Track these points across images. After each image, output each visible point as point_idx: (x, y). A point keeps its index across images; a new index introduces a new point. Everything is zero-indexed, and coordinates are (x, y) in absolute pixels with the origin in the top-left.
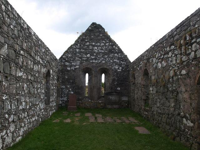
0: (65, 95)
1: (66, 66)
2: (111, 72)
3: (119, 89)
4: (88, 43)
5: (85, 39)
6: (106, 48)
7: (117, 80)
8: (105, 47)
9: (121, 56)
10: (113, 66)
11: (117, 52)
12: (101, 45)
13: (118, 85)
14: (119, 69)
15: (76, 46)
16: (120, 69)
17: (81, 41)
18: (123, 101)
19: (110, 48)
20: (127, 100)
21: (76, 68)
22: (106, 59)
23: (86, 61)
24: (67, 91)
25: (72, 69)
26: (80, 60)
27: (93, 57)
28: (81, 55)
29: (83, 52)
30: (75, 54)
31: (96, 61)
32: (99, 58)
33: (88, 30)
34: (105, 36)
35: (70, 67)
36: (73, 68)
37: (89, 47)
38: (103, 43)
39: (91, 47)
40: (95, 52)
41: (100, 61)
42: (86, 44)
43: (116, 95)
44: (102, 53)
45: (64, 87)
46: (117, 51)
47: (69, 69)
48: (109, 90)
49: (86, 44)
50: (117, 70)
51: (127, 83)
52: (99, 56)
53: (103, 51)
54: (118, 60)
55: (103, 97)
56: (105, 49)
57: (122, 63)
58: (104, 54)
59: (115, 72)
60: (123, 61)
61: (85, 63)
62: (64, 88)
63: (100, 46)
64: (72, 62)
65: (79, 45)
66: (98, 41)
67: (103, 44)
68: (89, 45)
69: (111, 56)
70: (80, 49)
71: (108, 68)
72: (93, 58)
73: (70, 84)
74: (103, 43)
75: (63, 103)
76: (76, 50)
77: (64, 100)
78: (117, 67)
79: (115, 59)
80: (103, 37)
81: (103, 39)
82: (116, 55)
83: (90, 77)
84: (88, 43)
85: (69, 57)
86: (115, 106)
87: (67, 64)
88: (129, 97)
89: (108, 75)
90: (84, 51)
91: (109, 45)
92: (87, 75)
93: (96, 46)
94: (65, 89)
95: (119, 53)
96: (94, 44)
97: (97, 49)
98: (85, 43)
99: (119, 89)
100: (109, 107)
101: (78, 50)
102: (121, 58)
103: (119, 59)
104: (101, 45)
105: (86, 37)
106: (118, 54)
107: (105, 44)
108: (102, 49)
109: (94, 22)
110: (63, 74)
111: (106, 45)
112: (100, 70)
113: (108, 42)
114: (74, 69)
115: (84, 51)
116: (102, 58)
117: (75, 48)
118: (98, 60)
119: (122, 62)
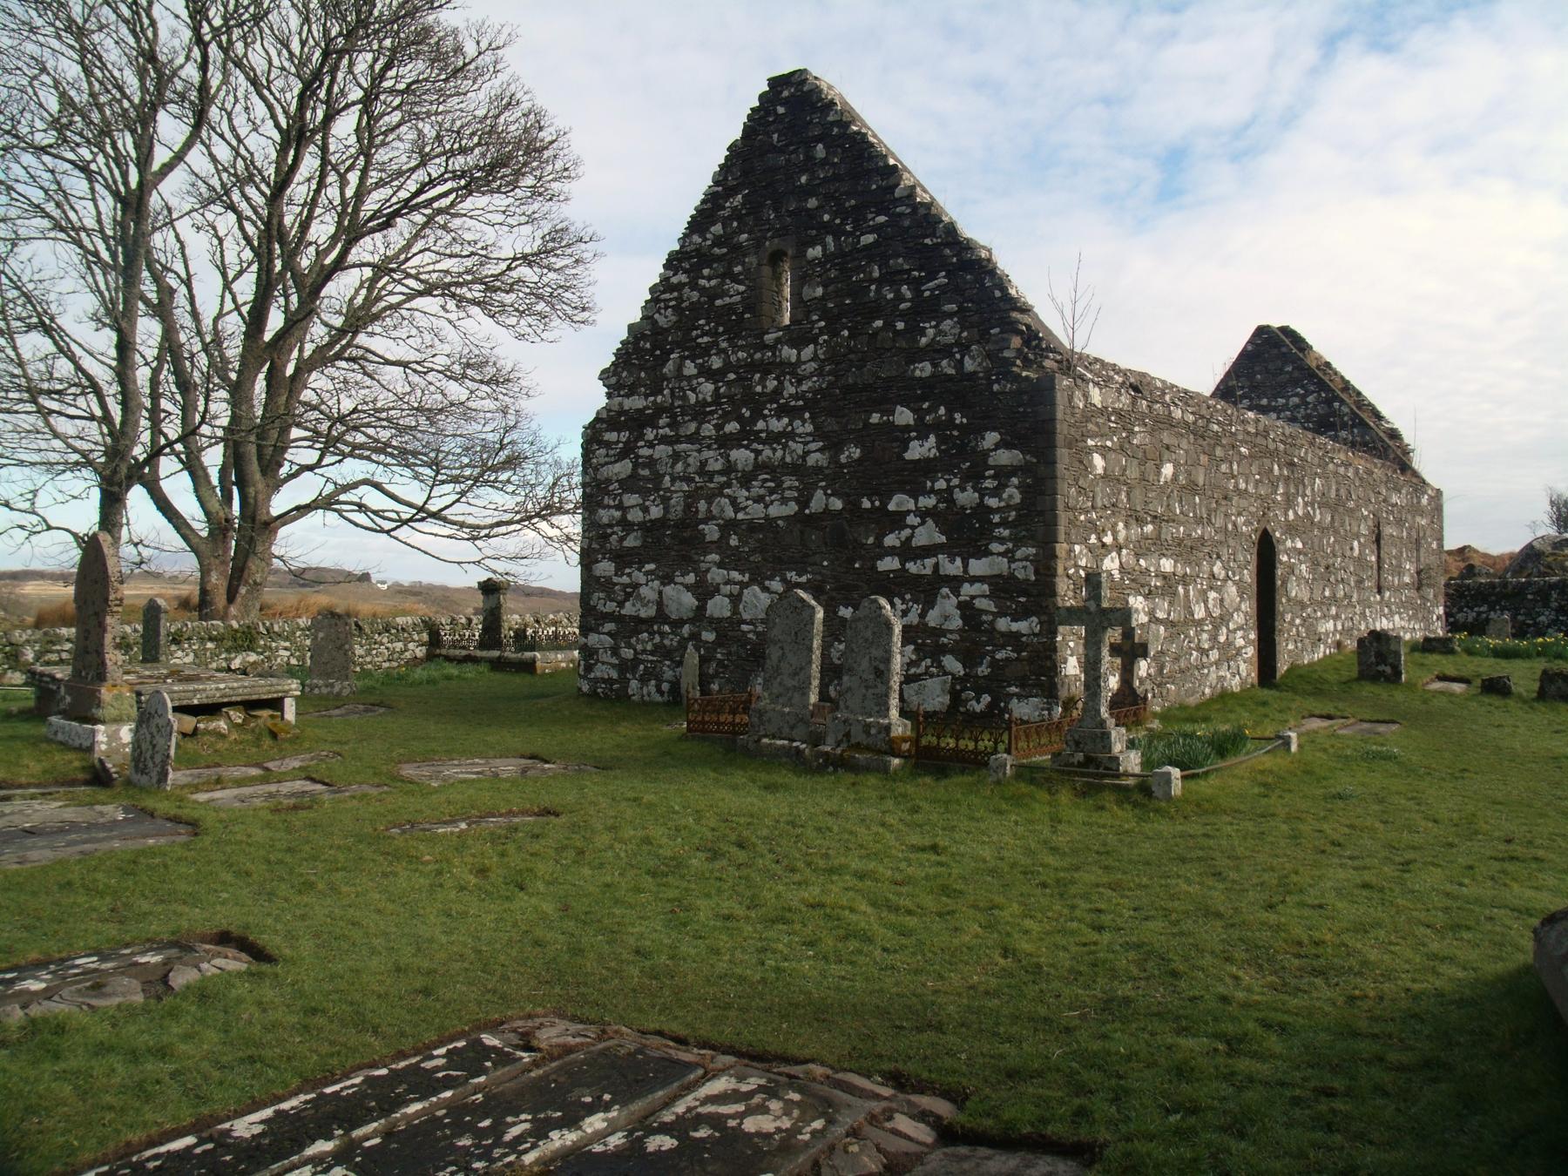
9: (1362, 437)
19: (1321, 412)
38: (1297, 395)
63: (1285, 407)
67: (1296, 400)
74: (1297, 395)
80: (1296, 374)
81: (1296, 383)
91: (1319, 401)
95: (1353, 426)
96: (1264, 402)
107: (1303, 397)
109: (1264, 323)
113: (1313, 392)
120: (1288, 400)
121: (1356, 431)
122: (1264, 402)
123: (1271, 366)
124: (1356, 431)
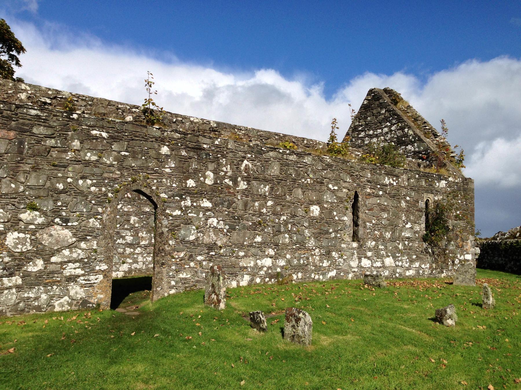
4: (362, 134)
6: (392, 135)
8: (391, 134)
9: (419, 147)
17: (353, 132)
34: (390, 111)
37: (363, 141)
42: (360, 136)
46: (411, 138)
49: (360, 136)
56: (389, 139)
63: (382, 134)
66: (379, 124)
81: (386, 119)
82: (409, 147)
93: (377, 136)
95: (415, 142)
96: (371, 132)
98: (358, 134)
102: (419, 152)
105: (359, 122)
106: (413, 146)
113: (395, 124)
120: (382, 130)
121: (416, 144)
122: (371, 132)
123: (375, 111)
124: (416, 144)
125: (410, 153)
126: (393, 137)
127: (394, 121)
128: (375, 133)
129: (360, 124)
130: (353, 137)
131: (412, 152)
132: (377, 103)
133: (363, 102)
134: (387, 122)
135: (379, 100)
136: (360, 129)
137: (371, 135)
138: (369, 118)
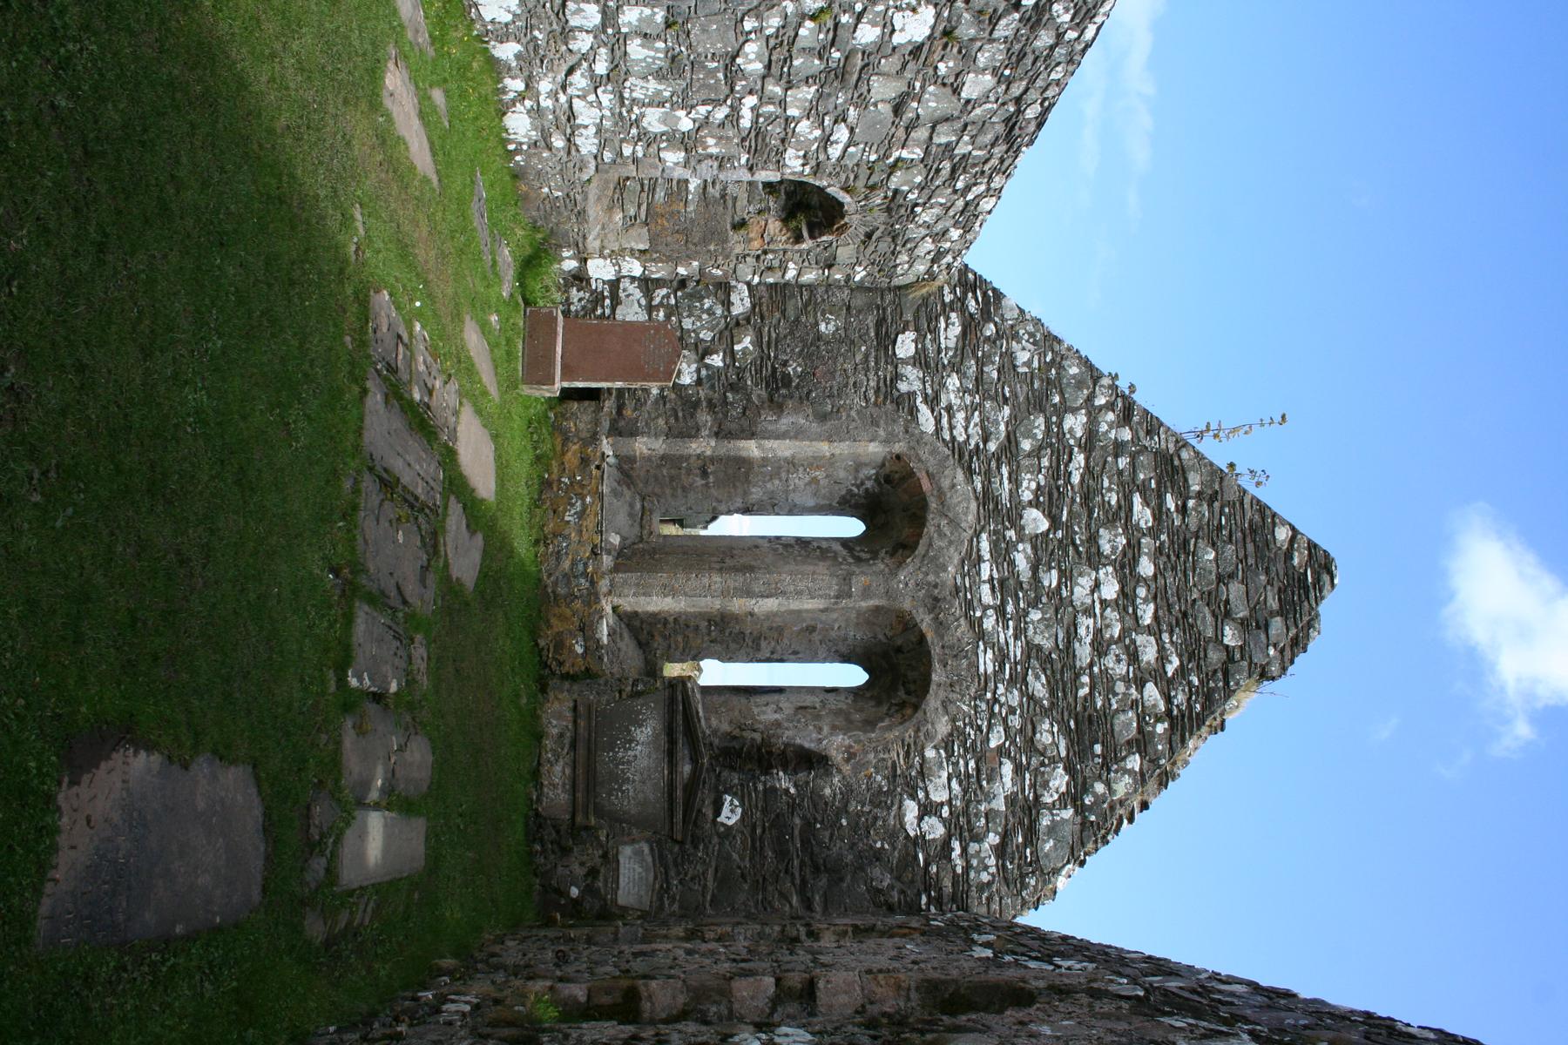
0: (668, 317)
1: (926, 321)
2: (894, 734)
3: (730, 815)
4: (1143, 515)
5: (1183, 495)
6: (1120, 687)
7: (816, 796)
9: (1053, 829)
10: (950, 754)
11: (1085, 788)
12: (1140, 639)
13: (765, 811)
14: (927, 809)
15: (1110, 406)
16: (920, 819)
18: (610, 859)
20: (621, 901)
21: (913, 411)
22: (1012, 681)
23: (987, 498)
24: (706, 335)
25: (897, 377)
26: (992, 446)
27: (1022, 562)
28: (1037, 453)
29: (1058, 472)
30: (1038, 403)
31: (986, 588)
32: (1021, 616)
33: (1266, 517)
35: (920, 360)
36: (912, 379)
38: (1162, 658)
39: (1111, 541)
40: (1067, 577)
41: (989, 623)
43: (671, 785)
44: (1068, 651)
45: (741, 303)
47: (906, 345)
48: (713, 724)
50: (913, 797)
51: (785, 897)
52: (1035, 615)
53: (1084, 652)
54: (1011, 800)
55: (652, 671)
56: (1105, 672)
57: (978, 839)
58: (1061, 668)
59: (893, 777)
60: (1000, 851)
61: (962, 492)
62: (727, 304)
63: (1133, 624)
64: (962, 375)
65: (1126, 434)
68: (1130, 528)
69: (1047, 734)
70: (1090, 441)
71: (933, 702)
72: (1012, 563)
73: (764, 357)
74: (1162, 658)
75: (598, 299)
76: (1074, 411)
77: (616, 301)
78: (939, 796)
79: (1019, 770)
80: (1215, 656)
81: (1193, 652)
82: (1059, 780)
83: (838, 547)
84: (1143, 515)
85: (1010, 356)
86: (558, 773)
87: (950, 332)
88: (653, 917)
89: (861, 710)
90: (1076, 479)
92: (852, 527)
93: (1126, 597)
94: (719, 311)
95: (1081, 810)
96: (1146, 568)
97: (1104, 603)
98: (1143, 489)
99: (730, 815)
100: (557, 716)
101: (1075, 423)
103: (1026, 810)
104: (1140, 639)
105: (1199, 495)
106: (1063, 801)
107: (1158, 674)
108: (1100, 646)
110: (859, 301)
111: (1141, 687)
112: (907, 624)
113: (1169, 700)
114: (903, 387)
115: (1076, 479)
116: (1016, 650)
117: (1090, 399)
118: (1001, 611)
119: (993, 839)
120: (1149, 630)
121: (1068, 813)
122: (1146, 568)
123: (1235, 590)
124: (1068, 813)
125: (1033, 786)
126: (1111, 691)
127: (1180, 698)
128: (1142, 592)
129: (1191, 503)
130: (1133, 457)
131: (1037, 797)
132: (1274, 604)
133: (1284, 522)
134: (1180, 656)
135: (1282, 612)
136: (1170, 502)
137: (1135, 561)
138: (1211, 556)
